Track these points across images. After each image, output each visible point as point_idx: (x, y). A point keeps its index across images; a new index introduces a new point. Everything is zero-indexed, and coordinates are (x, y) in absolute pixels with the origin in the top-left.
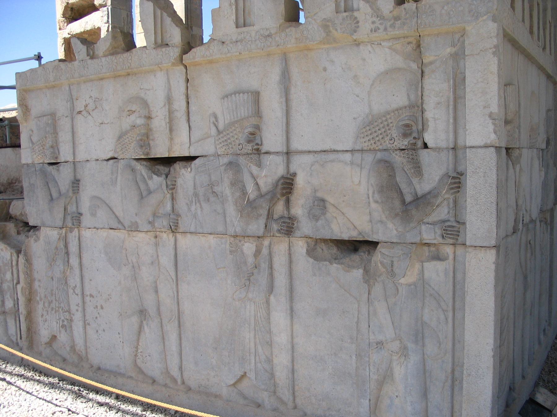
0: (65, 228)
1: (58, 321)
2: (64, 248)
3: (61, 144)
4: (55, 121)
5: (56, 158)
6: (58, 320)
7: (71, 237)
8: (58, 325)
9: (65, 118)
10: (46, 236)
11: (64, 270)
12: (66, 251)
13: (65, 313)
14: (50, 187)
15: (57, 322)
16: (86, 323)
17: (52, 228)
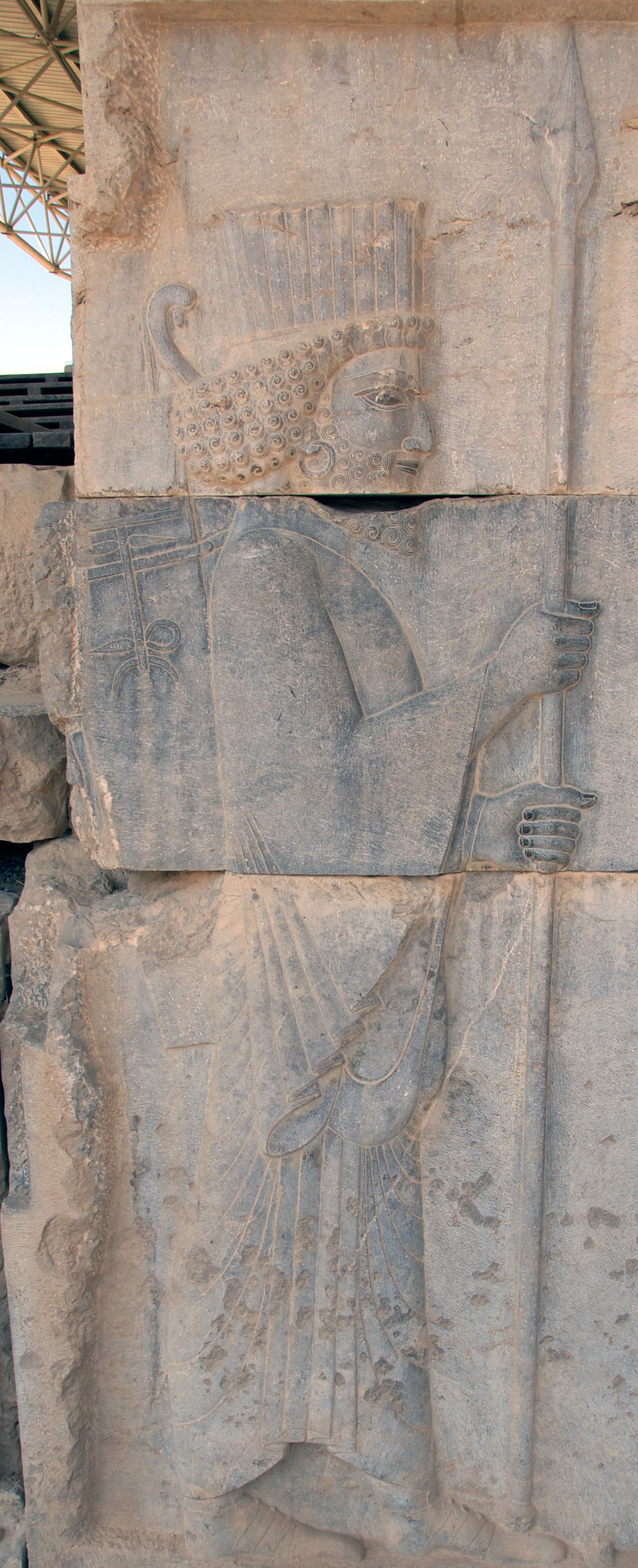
0: (449, 877)
1: (348, 1374)
2: (430, 985)
3: (451, 388)
4: (420, 244)
5: (413, 468)
6: (347, 1365)
7: (474, 924)
8: (342, 1393)
9: (501, 231)
10: (284, 927)
11: (416, 1101)
12: (439, 1006)
13: (397, 1327)
14: (347, 638)
15: (337, 1379)
16: (543, 1352)
17: (339, 881)
